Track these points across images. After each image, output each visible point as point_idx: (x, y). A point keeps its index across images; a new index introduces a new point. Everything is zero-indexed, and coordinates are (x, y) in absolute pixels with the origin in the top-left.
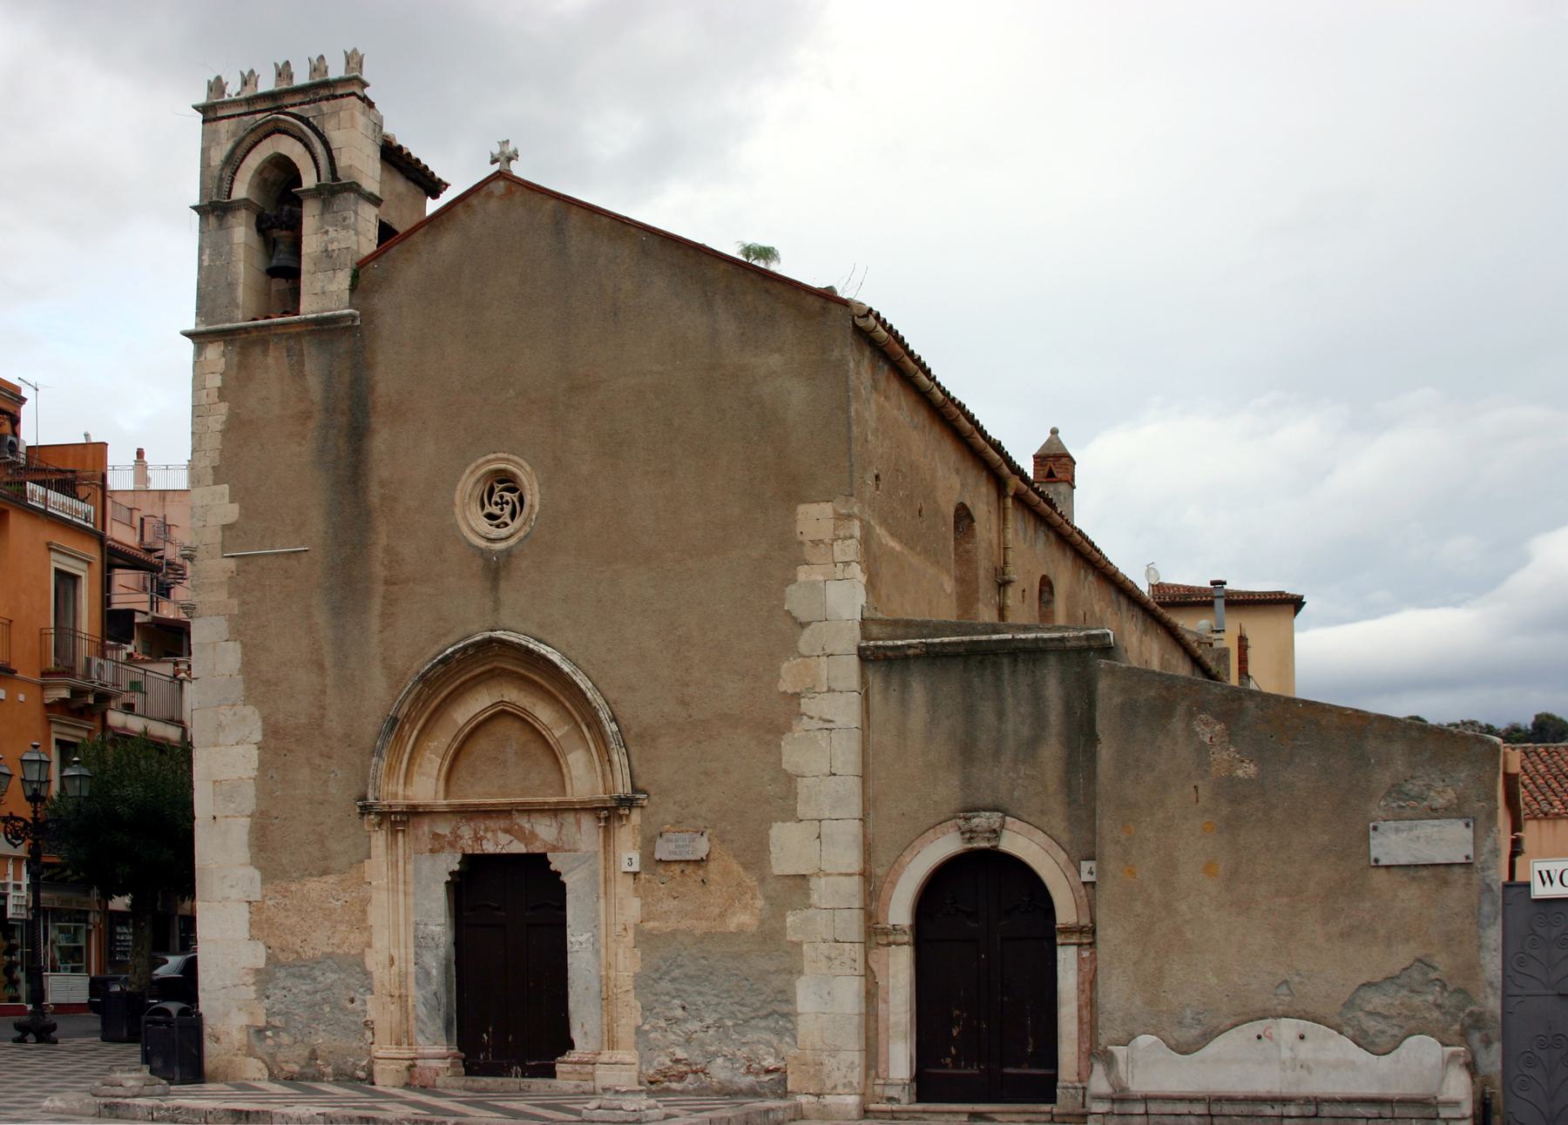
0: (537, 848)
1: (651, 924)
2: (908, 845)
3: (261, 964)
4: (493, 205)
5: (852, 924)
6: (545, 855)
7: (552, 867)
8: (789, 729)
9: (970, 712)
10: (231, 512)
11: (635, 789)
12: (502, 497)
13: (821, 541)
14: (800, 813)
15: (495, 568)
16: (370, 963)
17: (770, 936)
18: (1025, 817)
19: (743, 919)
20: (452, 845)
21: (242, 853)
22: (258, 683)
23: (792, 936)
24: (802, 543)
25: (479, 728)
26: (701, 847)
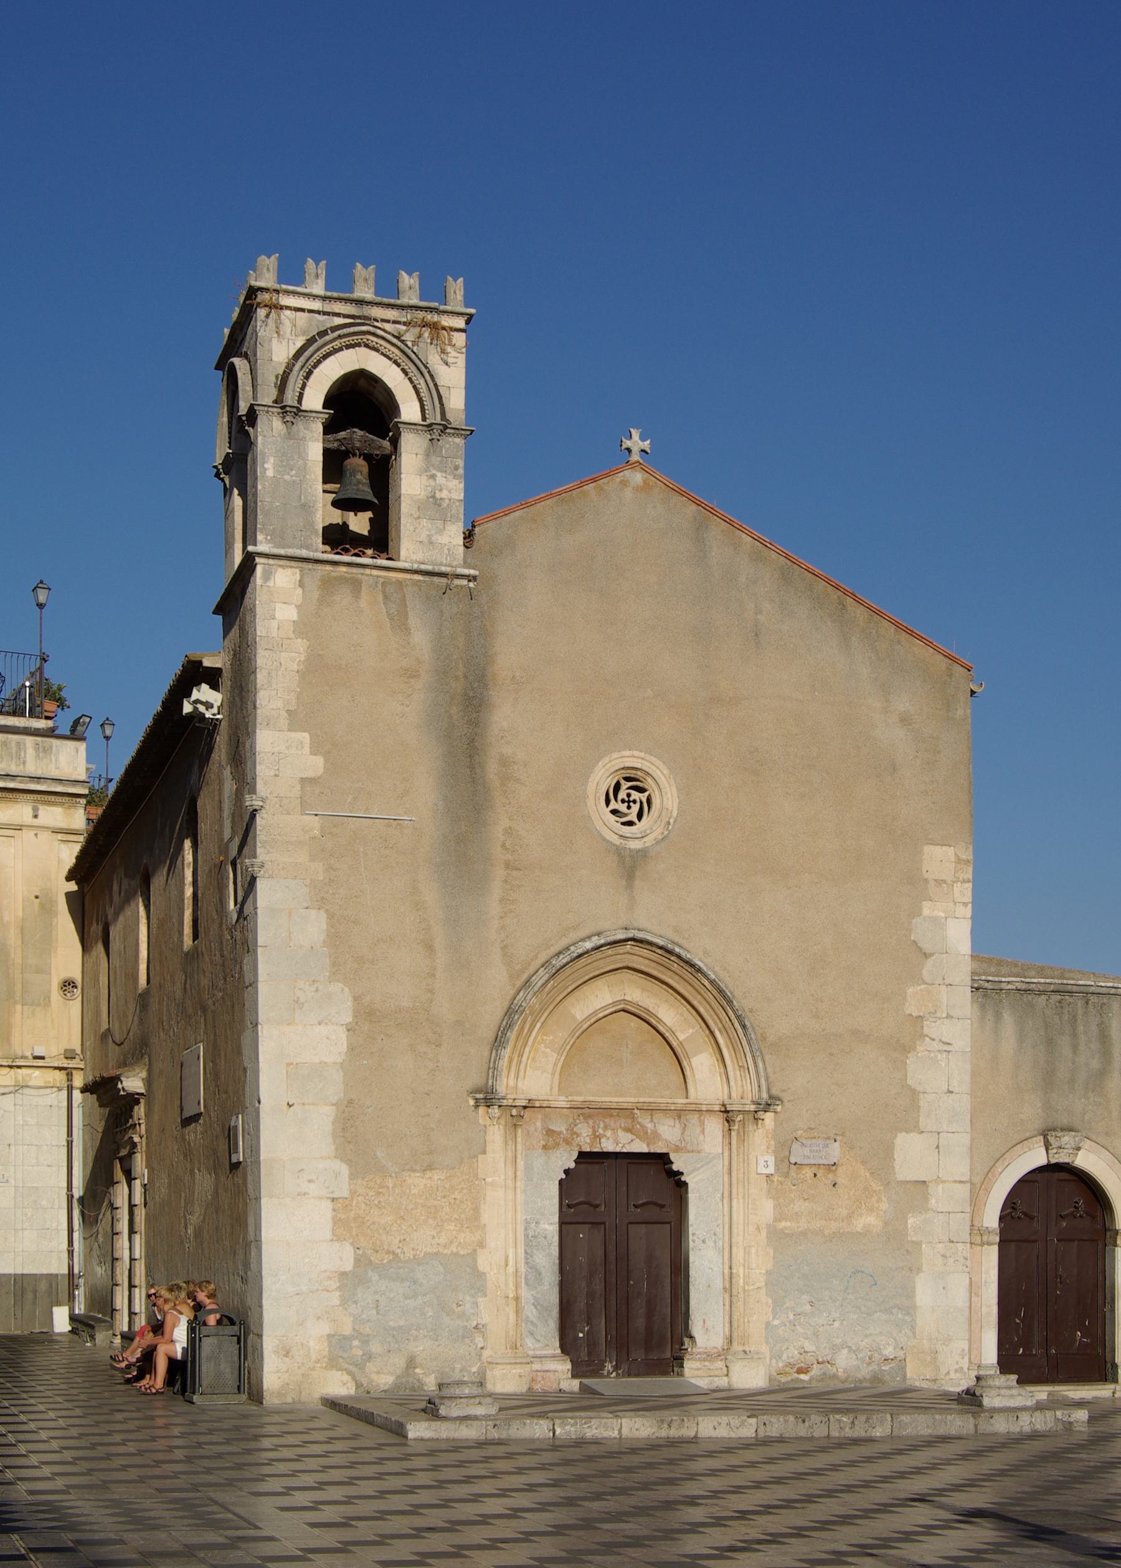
0: (659, 1148)
1: (784, 1224)
2: (1000, 1158)
3: (349, 1266)
4: (628, 494)
5: (960, 1224)
6: (667, 1154)
7: (675, 1167)
8: (914, 1049)
9: (1050, 1043)
10: (315, 765)
11: (771, 1097)
12: (629, 795)
13: (944, 882)
14: (922, 1121)
15: (631, 866)
16: (483, 1263)
17: (895, 1236)
18: (1094, 1137)
19: (867, 1221)
20: (568, 1142)
21: (326, 1146)
22: (346, 956)
23: (913, 1237)
24: (926, 881)
25: (598, 1021)
26: (835, 1152)
